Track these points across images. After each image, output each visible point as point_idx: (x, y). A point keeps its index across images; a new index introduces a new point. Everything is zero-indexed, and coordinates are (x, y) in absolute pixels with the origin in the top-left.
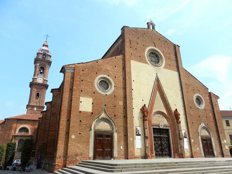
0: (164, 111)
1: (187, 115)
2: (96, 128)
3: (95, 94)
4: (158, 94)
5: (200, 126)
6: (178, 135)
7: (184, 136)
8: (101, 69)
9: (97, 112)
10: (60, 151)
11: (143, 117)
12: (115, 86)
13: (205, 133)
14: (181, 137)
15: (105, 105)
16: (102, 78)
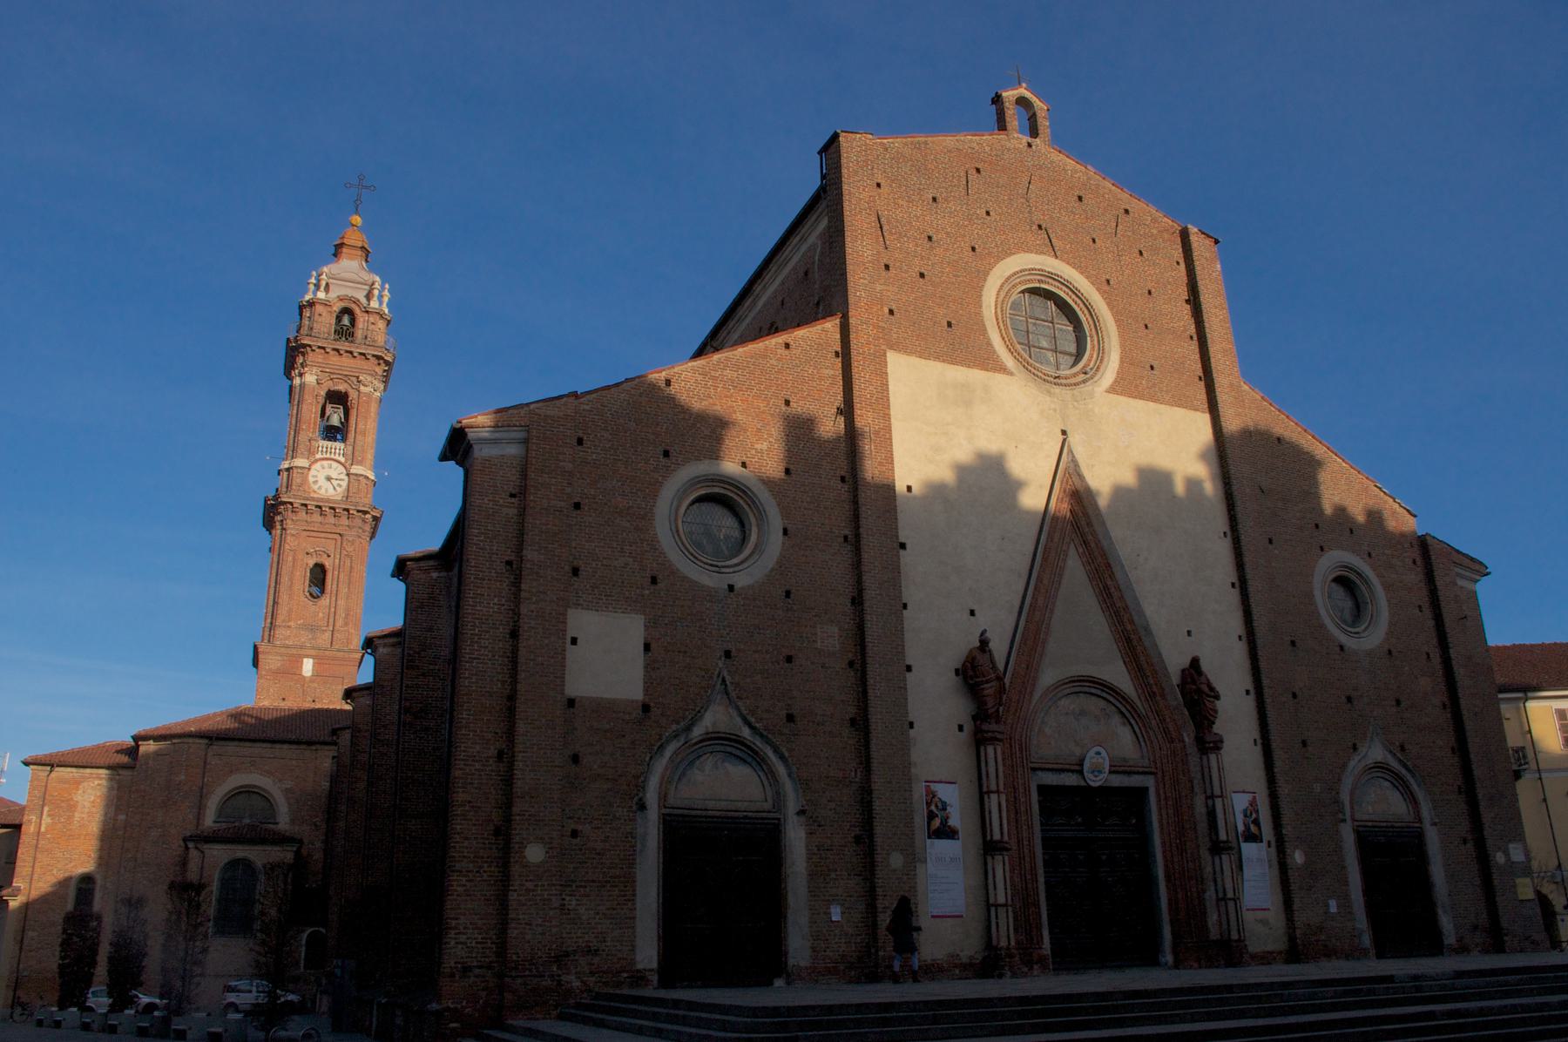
0: (1119, 677)
1: (1267, 691)
2: (671, 801)
3: (661, 585)
5: (1352, 763)
6: (1203, 826)
7: (1241, 828)
10: (463, 938)
11: (974, 718)
12: (785, 532)
13: (1383, 804)
14: (1223, 836)
15: (728, 654)
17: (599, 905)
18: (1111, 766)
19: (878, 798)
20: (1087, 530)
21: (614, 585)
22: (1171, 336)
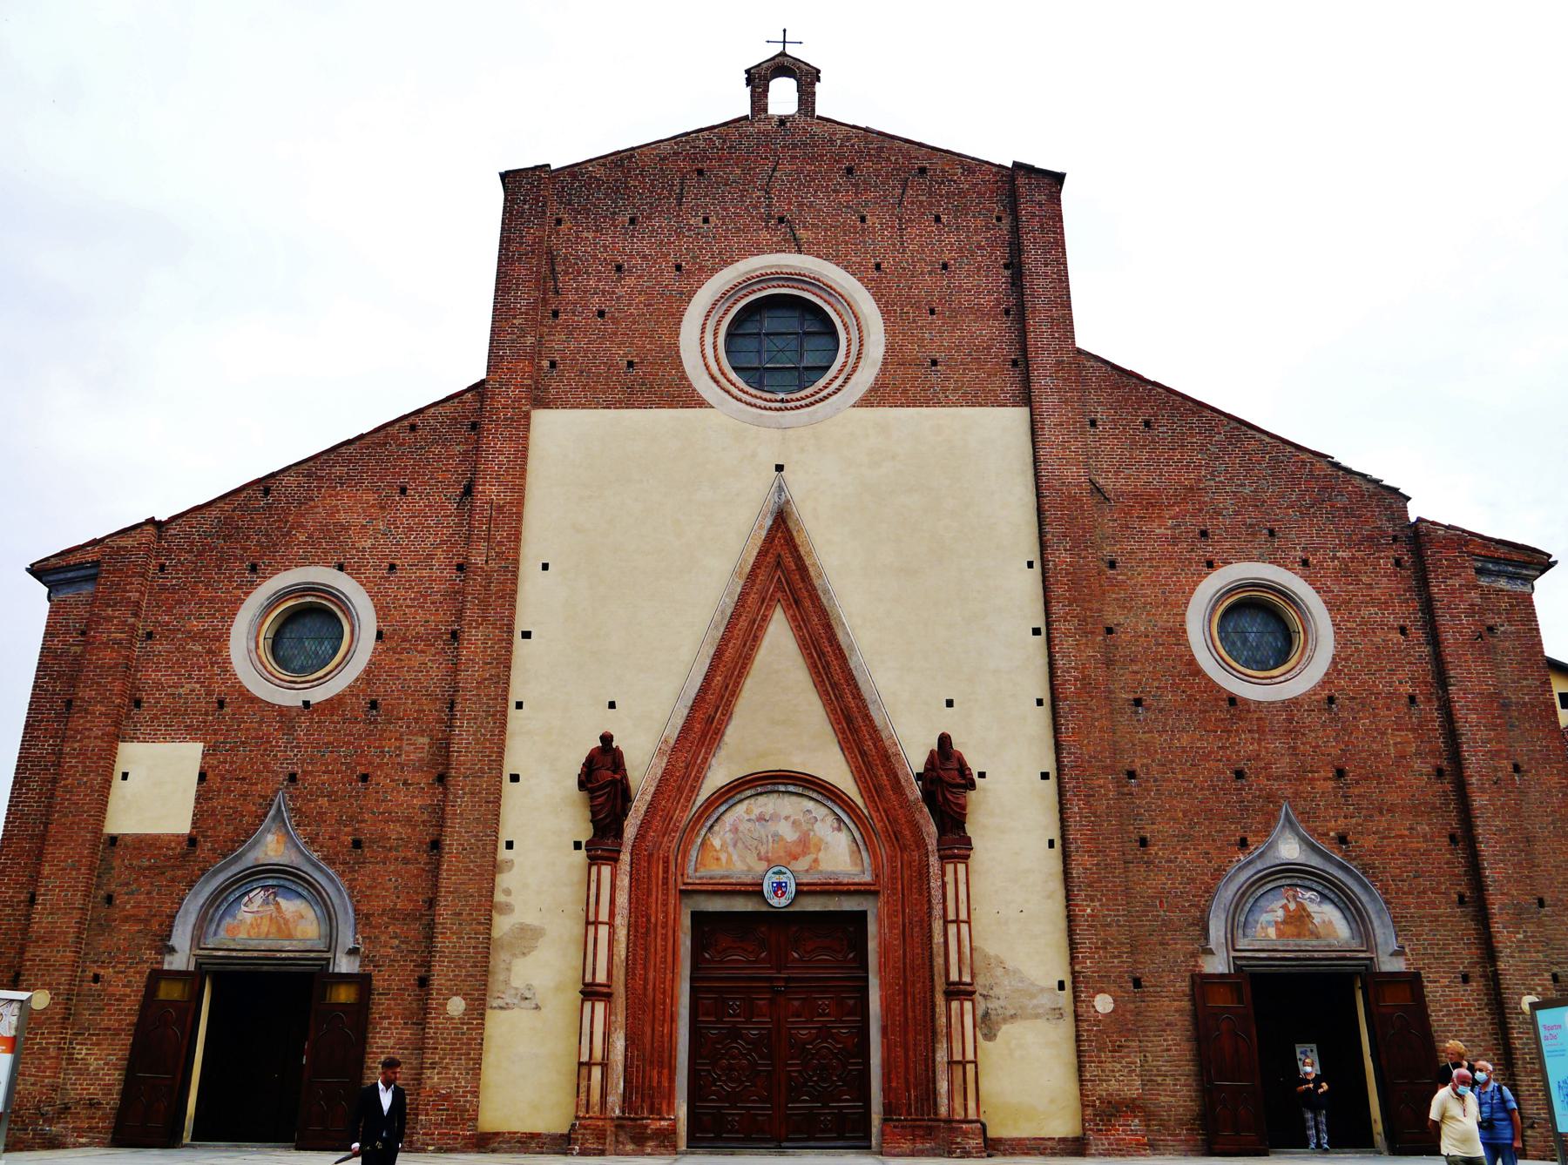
3: (227, 710)
4: (779, 638)
8: (289, 532)
9: (226, 830)
12: (380, 635)
15: (293, 778)
17: (109, 1055)
18: (797, 884)
19: (442, 933)
20: (801, 585)
22: (972, 317)
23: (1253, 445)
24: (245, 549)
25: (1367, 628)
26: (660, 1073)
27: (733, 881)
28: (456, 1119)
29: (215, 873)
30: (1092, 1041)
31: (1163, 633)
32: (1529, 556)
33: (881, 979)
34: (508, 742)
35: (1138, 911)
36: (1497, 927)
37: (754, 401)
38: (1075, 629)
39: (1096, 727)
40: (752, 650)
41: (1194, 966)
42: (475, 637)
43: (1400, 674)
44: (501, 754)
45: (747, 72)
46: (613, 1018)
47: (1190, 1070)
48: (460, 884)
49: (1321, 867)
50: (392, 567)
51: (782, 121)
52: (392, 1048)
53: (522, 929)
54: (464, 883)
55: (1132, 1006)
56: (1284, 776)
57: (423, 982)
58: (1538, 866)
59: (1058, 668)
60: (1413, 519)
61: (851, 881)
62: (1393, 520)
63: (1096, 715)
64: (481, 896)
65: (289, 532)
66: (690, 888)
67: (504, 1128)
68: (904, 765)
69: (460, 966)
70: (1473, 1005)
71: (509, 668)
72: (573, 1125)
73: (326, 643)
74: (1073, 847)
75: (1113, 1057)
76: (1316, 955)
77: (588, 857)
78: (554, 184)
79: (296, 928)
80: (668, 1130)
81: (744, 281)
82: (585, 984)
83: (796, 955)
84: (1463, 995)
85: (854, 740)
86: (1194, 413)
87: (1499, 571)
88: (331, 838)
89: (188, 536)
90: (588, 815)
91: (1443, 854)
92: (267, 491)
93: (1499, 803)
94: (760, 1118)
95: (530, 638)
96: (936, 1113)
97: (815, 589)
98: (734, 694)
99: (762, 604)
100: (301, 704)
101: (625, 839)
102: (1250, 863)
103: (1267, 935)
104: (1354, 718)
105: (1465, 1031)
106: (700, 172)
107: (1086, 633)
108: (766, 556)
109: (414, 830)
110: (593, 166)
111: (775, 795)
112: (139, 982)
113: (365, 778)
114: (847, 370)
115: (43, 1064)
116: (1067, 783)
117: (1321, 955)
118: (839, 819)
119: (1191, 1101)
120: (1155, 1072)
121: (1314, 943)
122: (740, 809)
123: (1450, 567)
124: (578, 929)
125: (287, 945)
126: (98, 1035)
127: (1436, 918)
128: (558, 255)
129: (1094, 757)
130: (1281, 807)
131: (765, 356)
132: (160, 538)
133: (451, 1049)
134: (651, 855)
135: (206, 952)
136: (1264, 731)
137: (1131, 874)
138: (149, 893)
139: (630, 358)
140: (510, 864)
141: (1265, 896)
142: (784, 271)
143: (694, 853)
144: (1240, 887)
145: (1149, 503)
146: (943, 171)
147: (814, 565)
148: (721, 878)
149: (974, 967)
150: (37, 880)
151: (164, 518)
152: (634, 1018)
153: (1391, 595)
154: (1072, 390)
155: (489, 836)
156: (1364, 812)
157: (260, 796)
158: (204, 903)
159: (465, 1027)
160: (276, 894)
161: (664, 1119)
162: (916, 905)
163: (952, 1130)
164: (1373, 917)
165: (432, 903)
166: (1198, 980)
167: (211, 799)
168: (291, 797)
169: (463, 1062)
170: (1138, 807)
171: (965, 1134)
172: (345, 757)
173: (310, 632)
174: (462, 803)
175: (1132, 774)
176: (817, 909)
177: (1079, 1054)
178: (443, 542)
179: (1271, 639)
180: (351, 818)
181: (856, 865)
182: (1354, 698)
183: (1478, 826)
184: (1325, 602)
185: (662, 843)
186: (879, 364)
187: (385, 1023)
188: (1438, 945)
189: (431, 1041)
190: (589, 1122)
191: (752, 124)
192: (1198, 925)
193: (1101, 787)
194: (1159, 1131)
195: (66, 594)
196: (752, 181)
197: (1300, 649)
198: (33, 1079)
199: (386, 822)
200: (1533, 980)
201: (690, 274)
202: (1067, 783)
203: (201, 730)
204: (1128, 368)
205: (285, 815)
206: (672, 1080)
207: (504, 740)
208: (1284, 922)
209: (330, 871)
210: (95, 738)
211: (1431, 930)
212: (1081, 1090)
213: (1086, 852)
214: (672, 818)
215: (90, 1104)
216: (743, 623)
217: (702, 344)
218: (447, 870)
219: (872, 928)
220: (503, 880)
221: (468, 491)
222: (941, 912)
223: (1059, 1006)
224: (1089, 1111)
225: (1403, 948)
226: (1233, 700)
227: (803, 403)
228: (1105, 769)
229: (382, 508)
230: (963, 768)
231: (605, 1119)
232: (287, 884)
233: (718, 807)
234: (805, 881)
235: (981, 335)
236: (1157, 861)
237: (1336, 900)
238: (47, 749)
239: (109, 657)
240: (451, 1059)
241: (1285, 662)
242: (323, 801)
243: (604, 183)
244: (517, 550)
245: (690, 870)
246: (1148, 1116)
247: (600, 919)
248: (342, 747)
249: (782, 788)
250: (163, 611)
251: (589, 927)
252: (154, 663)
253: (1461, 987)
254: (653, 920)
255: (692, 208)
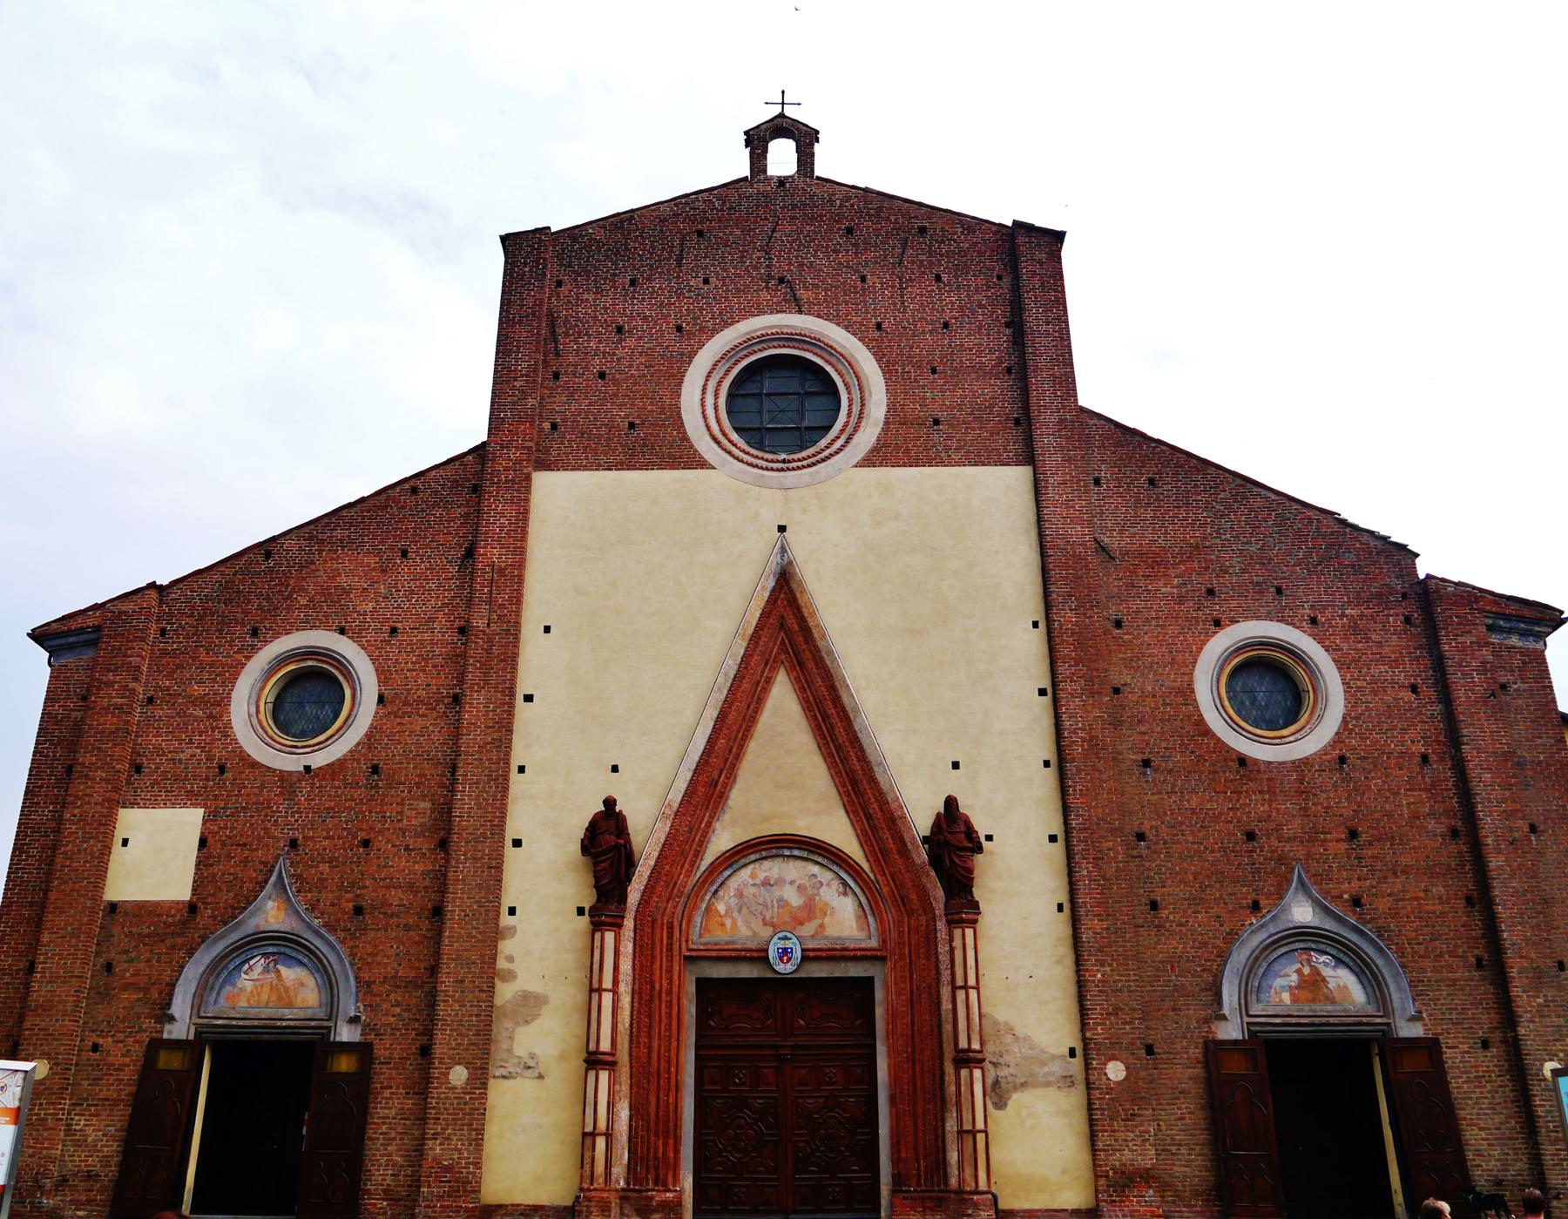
3: (228, 775)
8: (290, 596)
9: (226, 897)
12: (381, 699)
15: (294, 844)
16: (282, 661)
17: (108, 1126)
18: (803, 950)
19: (444, 1001)
20: (804, 647)
21: (175, 780)
22: (973, 376)
23: (1259, 502)
24: (245, 613)
25: (1378, 687)
26: (665, 1144)
27: (738, 947)
28: (459, 1191)
29: (216, 941)
30: (1104, 1109)
31: (1170, 693)
32: (1540, 612)
33: (888, 1047)
34: (510, 807)
35: (1149, 976)
36: (1516, 991)
37: (755, 461)
38: (1082, 689)
39: (1103, 789)
40: (756, 712)
41: (1207, 1032)
42: (477, 702)
43: (1412, 734)
44: (503, 819)
45: (746, 133)
46: (617, 1087)
47: (1204, 1139)
48: (463, 950)
49: (1335, 930)
50: (394, 630)
51: (782, 181)
52: (393, 1118)
53: (525, 996)
54: (466, 950)
55: (1143, 1074)
56: (1295, 838)
57: (426, 1051)
58: (1557, 928)
59: (1065, 729)
60: (1422, 576)
61: (857, 946)
62: (1402, 576)
63: (1104, 777)
64: (485, 963)
65: (290, 596)
66: (694, 954)
67: (507, 1200)
68: (910, 828)
69: (462, 1035)
70: (1493, 1072)
71: (511, 731)
72: (578, 1197)
73: (327, 707)
74: (1082, 911)
75: (1125, 1126)
76: (1331, 1020)
77: (592, 922)
78: (554, 246)
79: (296, 997)
80: (673, 1202)
81: (745, 342)
82: (588, 1052)
83: (802, 1022)
84: (1483, 1062)
85: (859, 803)
86: (1198, 470)
87: (1511, 628)
88: (333, 905)
89: (189, 600)
90: (592, 881)
91: (1460, 917)
92: (268, 555)
93: (1515, 864)
94: (767, 1190)
95: (532, 701)
96: (946, 1183)
97: (818, 650)
98: (738, 757)
99: (766, 665)
100: (302, 769)
101: (628, 905)
102: (1262, 926)
103: (1281, 1001)
104: (1366, 778)
105: (1486, 1098)
106: (700, 233)
107: (1092, 694)
108: (769, 617)
109: (415, 896)
110: (593, 229)
111: (781, 859)
112: (138, 1051)
113: (366, 843)
114: (849, 429)
115: (41, 1135)
116: (1076, 846)
117: (1336, 1020)
118: (845, 884)
119: (1206, 1171)
120: (1169, 1141)
121: (1329, 1008)
122: (745, 874)
123: (1461, 624)
124: (582, 997)
125: (287, 1013)
126: (97, 1105)
127: (1454, 982)
128: (559, 317)
129: (1103, 820)
130: (1293, 869)
131: (766, 416)
132: (161, 602)
133: (454, 1120)
134: (654, 921)
135: (206, 1021)
136: (1274, 792)
137: (1141, 938)
138: (148, 961)
139: (631, 420)
140: (512, 930)
141: (1279, 961)
142: (785, 331)
143: (698, 919)
144: (1253, 952)
145: (1155, 562)
146: (943, 230)
147: (818, 626)
148: (726, 944)
149: (984, 1033)
150: (36, 949)
151: (165, 582)
152: (638, 1087)
153: (1401, 653)
154: (1075, 449)
155: (491, 902)
156: (1378, 874)
157: (261, 862)
158: (205, 971)
159: (468, 1097)
160: (276, 962)
161: (669, 1191)
162: (924, 970)
163: (963, 1201)
164: (1389, 980)
165: (433, 970)
166: (1212, 1047)
167: (212, 865)
168: (292, 863)
169: (465, 1132)
170: (1148, 869)
171: (976, 1206)
172: (346, 822)
173: (311, 696)
174: (463, 868)
175: (1141, 837)
176: (823, 975)
177: (1092, 1122)
178: (444, 605)
179: (1280, 699)
180: (352, 884)
181: (862, 930)
182: (1365, 758)
183: (1495, 887)
184: (1334, 661)
185: (666, 909)
186: (881, 424)
187: (387, 1093)
188: (1457, 1009)
189: (433, 1111)
190: (593, 1194)
191: (752, 185)
192: (1210, 990)
193: (1109, 849)
194: (1174, 1202)
195: (68, 659)
196: (752, 242)
197: (1310, 709)
198: (31, 1150)
199: (388, 888)
200: (1554, 1045)
201: (692, 336)
202: (1076, 846)
203: (202, 795)
204: (1132, 426)
205: (286, 881)
206: (677, 1150)
207: (506, 805)
208: (1299, 987)
209: (331, 938)
210: (95, 804)
211: (1448, 995)
212: (1094, 1160)
213: (1095, 916)
214: (676, 883)
215: (88, 1176)
216: (746, 686)
217: (703, 405)
218: (449, 937)
219: (879, 995)
220: (506, 947)
221: (470, 553)
222: (949, 979)
223: (1070, 1073)
224: (1102, 1181)
225: (1420, 1012)
226: (1242, 760)
227: (805, 463)
228: (1113, 831)
229: (384, 571)
230: (970, 831)
231: (610, 1190)
232: (288, 951)
233: (722, 872)
234: (810, 946)
235: (983, 394)
236: (1168, 925)
237: (1351, 964)
238: (47, 816)
239: (110, 722)
240: (453, 1129)
241: (1294, 721)
242: (325, 867)
243: (604, 245)
244: (518, 613)
245: (694, 936)
246: (1163, 1187)
247: (604, 986)
248: (343, 812)
249: (787, 852)
250: (164, 676)
251: (593, 995)
252: (154, 728)
253: (1481, 1053)
254: (657, 987)
255: (692, 269)
